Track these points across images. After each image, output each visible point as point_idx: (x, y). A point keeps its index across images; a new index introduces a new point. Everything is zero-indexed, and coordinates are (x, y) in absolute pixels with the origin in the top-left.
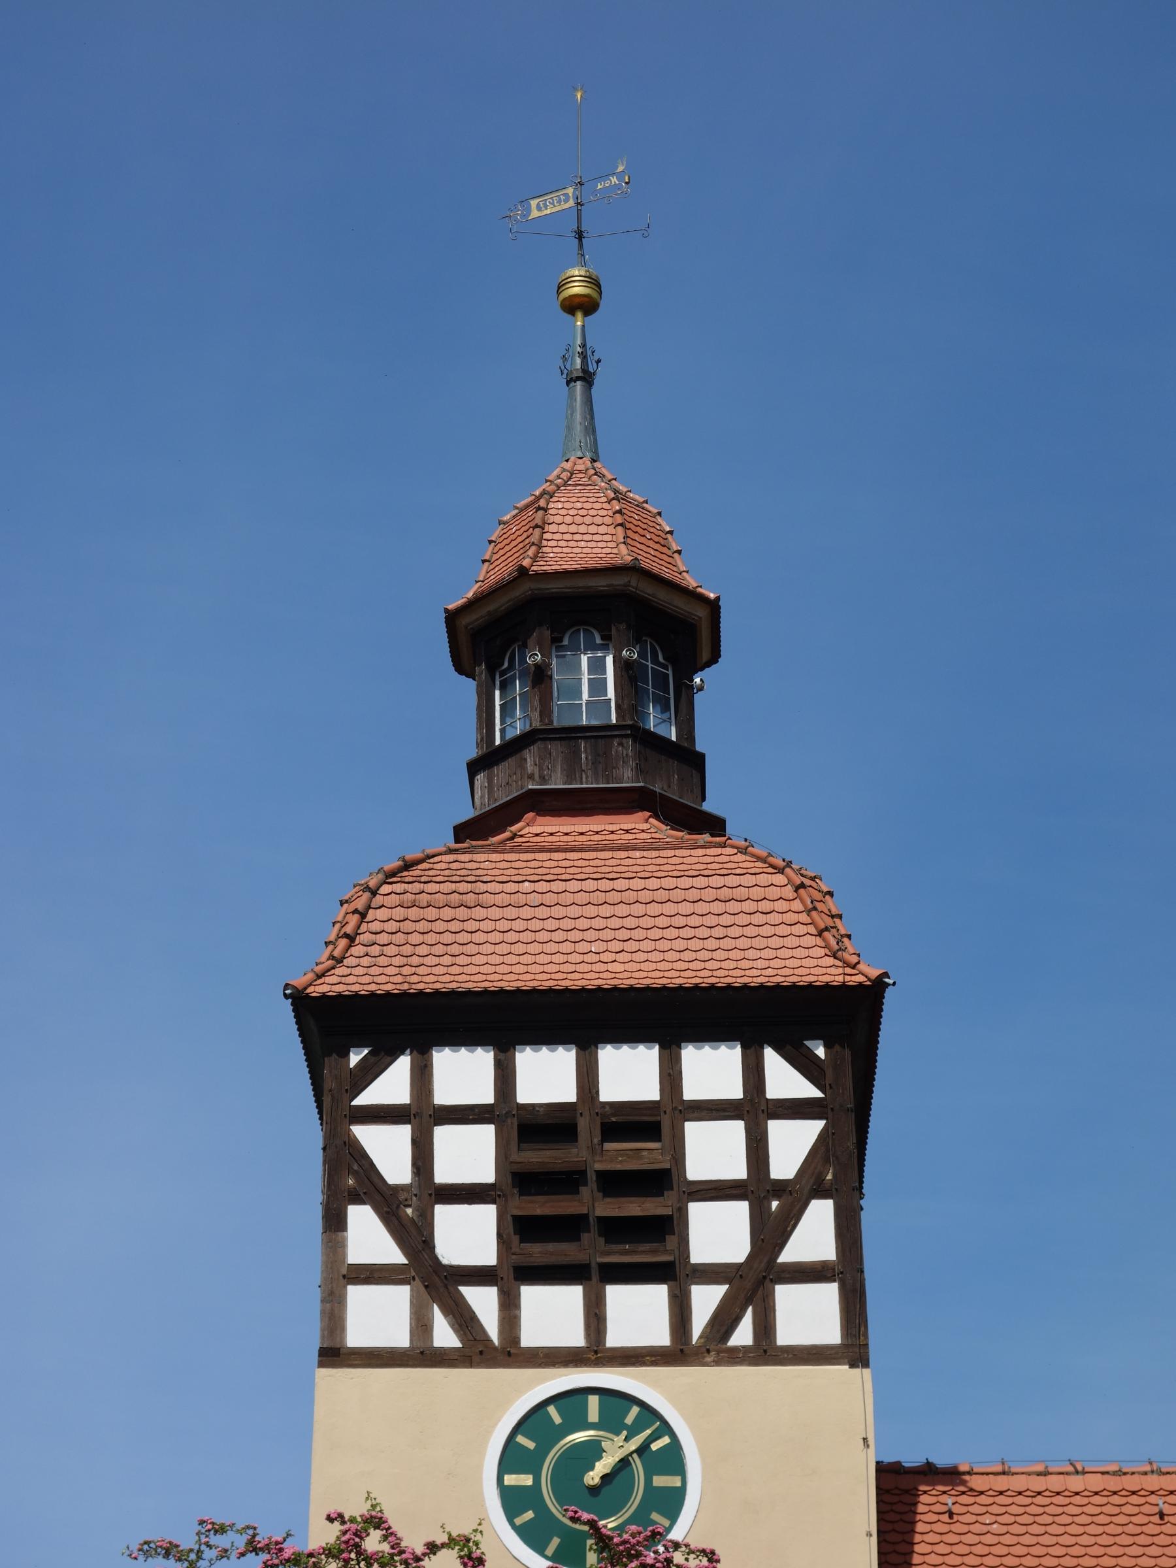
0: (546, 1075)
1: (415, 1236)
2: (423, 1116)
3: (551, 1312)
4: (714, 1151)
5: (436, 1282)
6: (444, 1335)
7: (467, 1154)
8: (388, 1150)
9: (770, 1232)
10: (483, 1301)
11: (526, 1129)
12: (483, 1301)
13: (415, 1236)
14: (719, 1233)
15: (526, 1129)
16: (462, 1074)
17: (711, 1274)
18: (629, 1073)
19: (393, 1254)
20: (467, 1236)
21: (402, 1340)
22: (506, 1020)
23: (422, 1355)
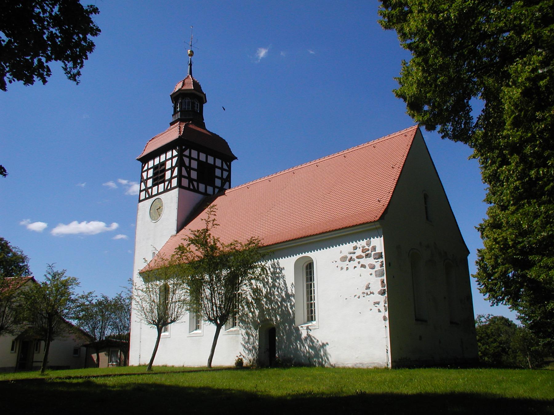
0: (203, 157)
1: (189, 173)
2: (190, 158)
3: (202, 187)
4: (218, 172)
5: (191, 180)
6: (191, 187)
7: (194, 164)
8: (186, 160)
9: (223, 184)
10: (195, 184)
11: (199, 162)
12: (195, 184)
13: (189, 173)
14: (218, 182)
15: (199, 162)
16: (194, 154)
17: (218, 187)
18: (211, 160)
20: (194, 175)
21: (187, 186)
22: (200, 150)
23: (188, 189)
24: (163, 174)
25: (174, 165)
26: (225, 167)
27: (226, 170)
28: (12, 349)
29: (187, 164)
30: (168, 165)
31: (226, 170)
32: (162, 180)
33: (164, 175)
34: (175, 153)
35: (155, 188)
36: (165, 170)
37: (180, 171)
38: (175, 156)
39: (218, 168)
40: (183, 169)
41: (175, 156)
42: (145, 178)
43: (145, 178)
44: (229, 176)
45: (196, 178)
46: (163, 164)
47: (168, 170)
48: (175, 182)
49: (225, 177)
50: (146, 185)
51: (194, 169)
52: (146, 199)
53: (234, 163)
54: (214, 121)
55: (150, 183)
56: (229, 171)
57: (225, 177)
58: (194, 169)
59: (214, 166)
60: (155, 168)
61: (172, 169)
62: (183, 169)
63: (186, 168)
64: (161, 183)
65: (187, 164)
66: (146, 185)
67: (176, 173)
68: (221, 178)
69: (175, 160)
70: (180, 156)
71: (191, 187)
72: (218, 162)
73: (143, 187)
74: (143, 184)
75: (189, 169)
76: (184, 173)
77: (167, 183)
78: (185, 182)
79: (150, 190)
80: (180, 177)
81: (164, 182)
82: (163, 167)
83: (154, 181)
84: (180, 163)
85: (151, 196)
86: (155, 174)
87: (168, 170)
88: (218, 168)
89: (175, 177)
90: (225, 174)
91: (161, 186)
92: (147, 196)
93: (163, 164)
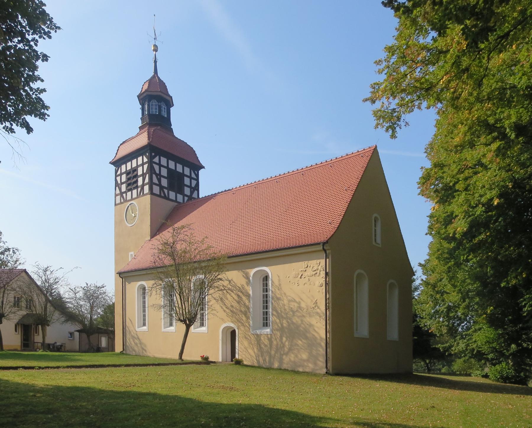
1: (159, 180)
3: (172, 195)
4: (187, 181)
5: (162, 188)
6: (162, 195)
7: (164, 172)
10: (166, 191)
13: (159, 180)
19: (157, 183)
20: (164, 182)
23: (160, 196)
24: (135, 180)
25: (145, 172)
26: (193, 176)
27: (194, 179)
28: (16, 331)
29: (158, 172)
30: (140, 172)
31: (194, 179)
32: (135, 185)
33: (137, 181)
34: (146, 160)
35: (129, 194)
36: (136, 176)
37: (151, 179)
38: (146, 163)
39: (187, 176)
40: (154, 176)
41: (146, 163)
42: (119, 182)
43: (119, 182)
44: (197, 185)
45: (166, 186)
46: (135, 170)
47: (140, 176)
48: (146, 189)
49: (193, 185)
50: (120, 189)
51: (164, 177)
52: (121, 203)
53: (201, 172)
54: (184, 126)
55: (124, 188)
56: (197, 180)
57: (193, 185)
58: (164, 177)
59: (182, 175)
60: (128, 173)
61: (143, 175)
62: (154, 176)
63: (157, 175)
64: (134, 188)
65: (158, 172)
66: (120, 189)
67: (147, 180)
68: (190, 187)
69: (146, 166)
70: (151, 163)
71: (162, 195)
72: (187, 171)
73: (118, 192)
74: (117, 188)
75: (159, 176)
76: (155, 180)
77: (139, 189)
78: (156, 190)
79: (124, 195)
80: (151, 184)
81: (137, 187)
82: (136, 173)
83: (129, 185)
84: (151, 170)
85: (126, 201)
86: (129, 179)
87: (140, 176)
88: (187, 176)
89: (146, 184)
90: (194, 183)
91: (135, 192)
92: (122, 201)
93: (135, 170)
